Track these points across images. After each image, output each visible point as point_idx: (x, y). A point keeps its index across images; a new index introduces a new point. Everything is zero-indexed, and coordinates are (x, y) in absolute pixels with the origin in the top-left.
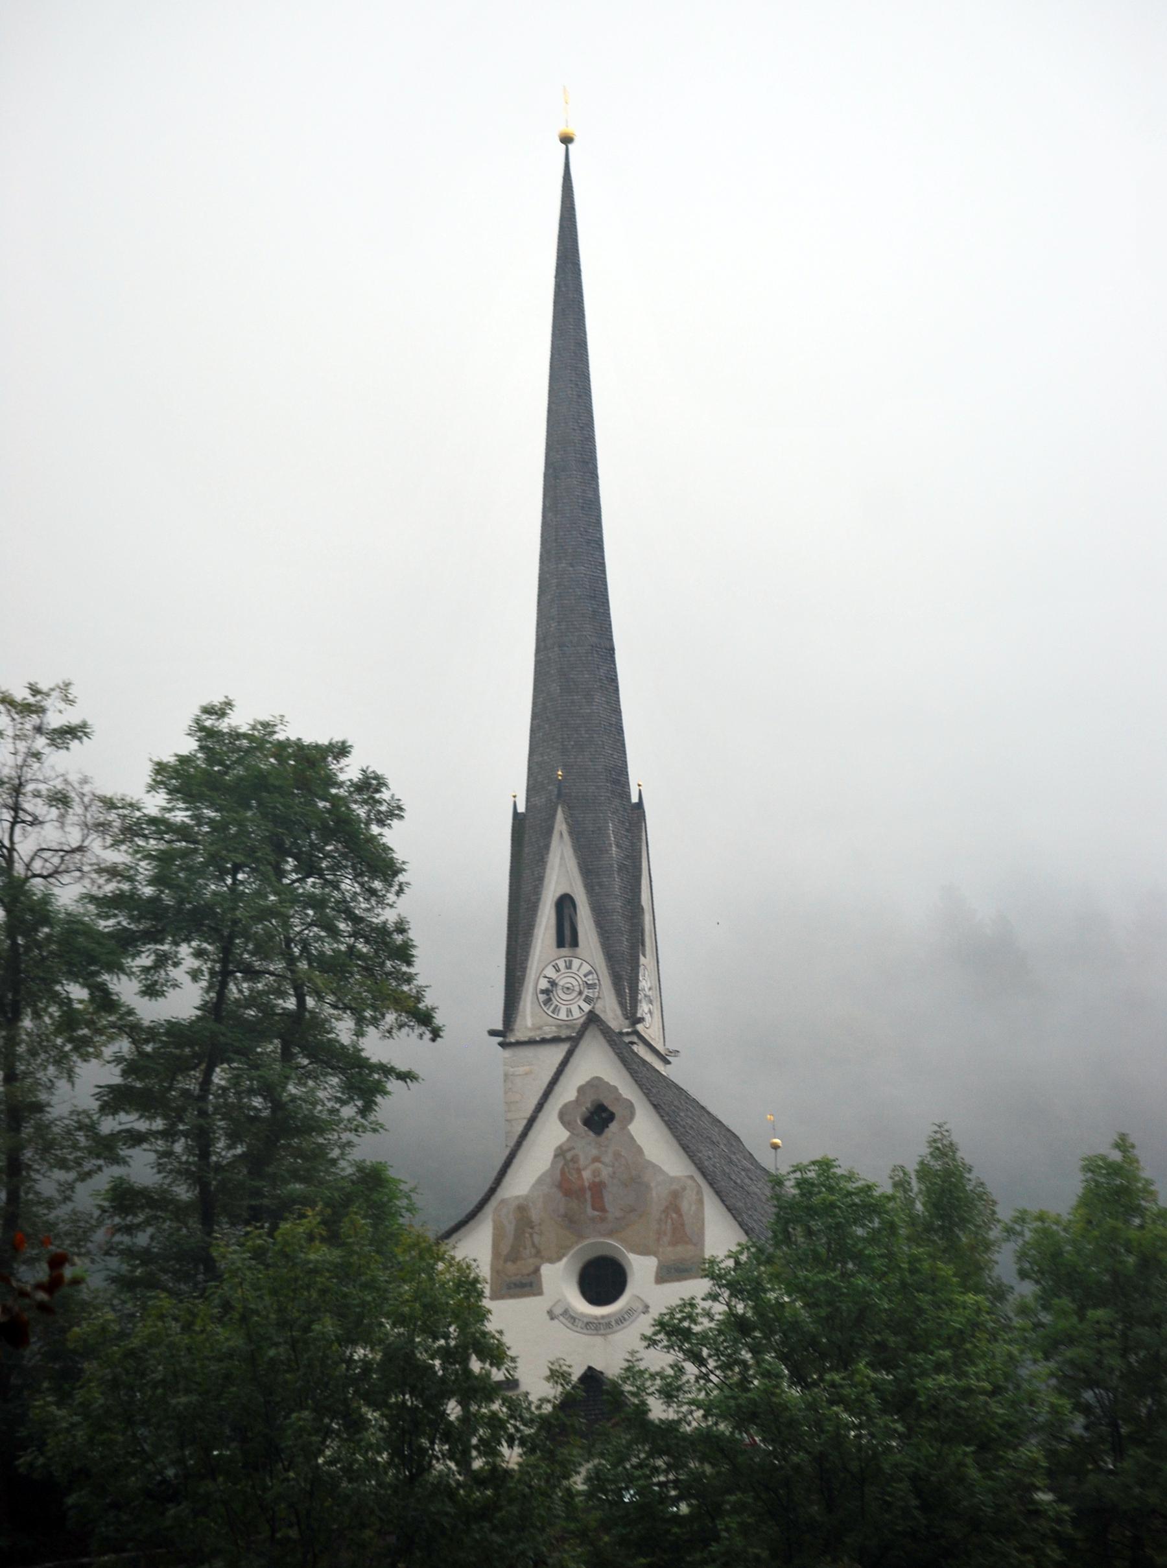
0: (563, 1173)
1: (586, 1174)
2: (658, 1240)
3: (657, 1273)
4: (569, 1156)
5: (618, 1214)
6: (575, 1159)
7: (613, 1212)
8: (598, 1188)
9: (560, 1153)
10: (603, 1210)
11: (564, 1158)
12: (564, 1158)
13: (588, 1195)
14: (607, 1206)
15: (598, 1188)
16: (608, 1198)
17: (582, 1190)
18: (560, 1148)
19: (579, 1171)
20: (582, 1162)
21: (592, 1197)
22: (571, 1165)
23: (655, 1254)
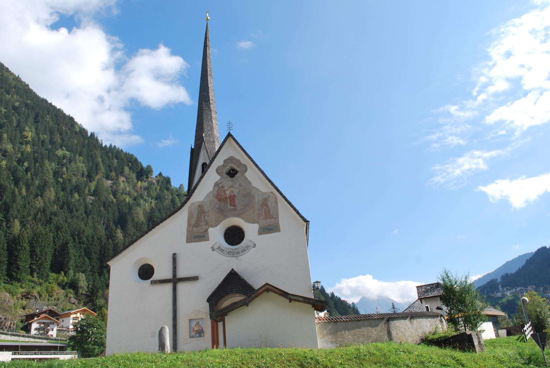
0: (218, 192)
1: (228, 192)
2: (259, 217)
3: (259, 231)
4: (220, 185)
5: (241, 207)
6: (223, 187)
7: (239, 206)
8: (232, 198)
9: (217, 184)
10: (235, 206)
11: (218, 186)
12: (218, 186)
13: (229, 200)
14: (237, 204)
15: (232, 198)
16: (237, 201)
17: (226, 198)
18: (217, 182)
19: (224, 191)
20: (226, 188)
21: (230, 201)
22: (221, 189)
23: (258, 223)
